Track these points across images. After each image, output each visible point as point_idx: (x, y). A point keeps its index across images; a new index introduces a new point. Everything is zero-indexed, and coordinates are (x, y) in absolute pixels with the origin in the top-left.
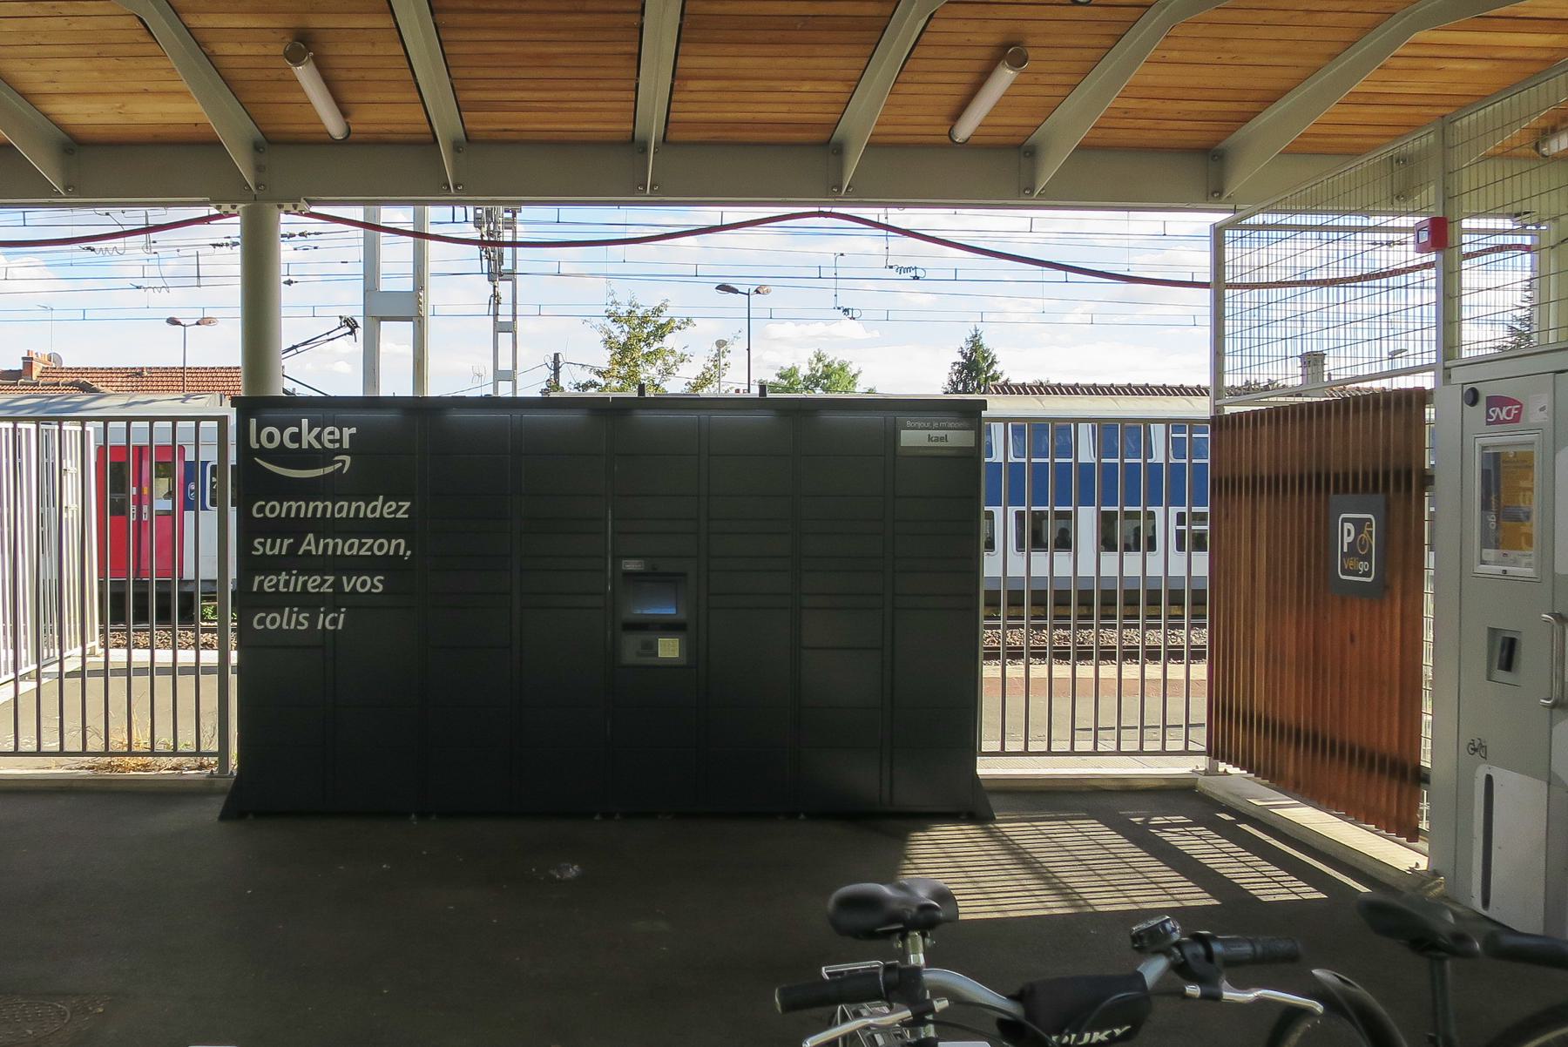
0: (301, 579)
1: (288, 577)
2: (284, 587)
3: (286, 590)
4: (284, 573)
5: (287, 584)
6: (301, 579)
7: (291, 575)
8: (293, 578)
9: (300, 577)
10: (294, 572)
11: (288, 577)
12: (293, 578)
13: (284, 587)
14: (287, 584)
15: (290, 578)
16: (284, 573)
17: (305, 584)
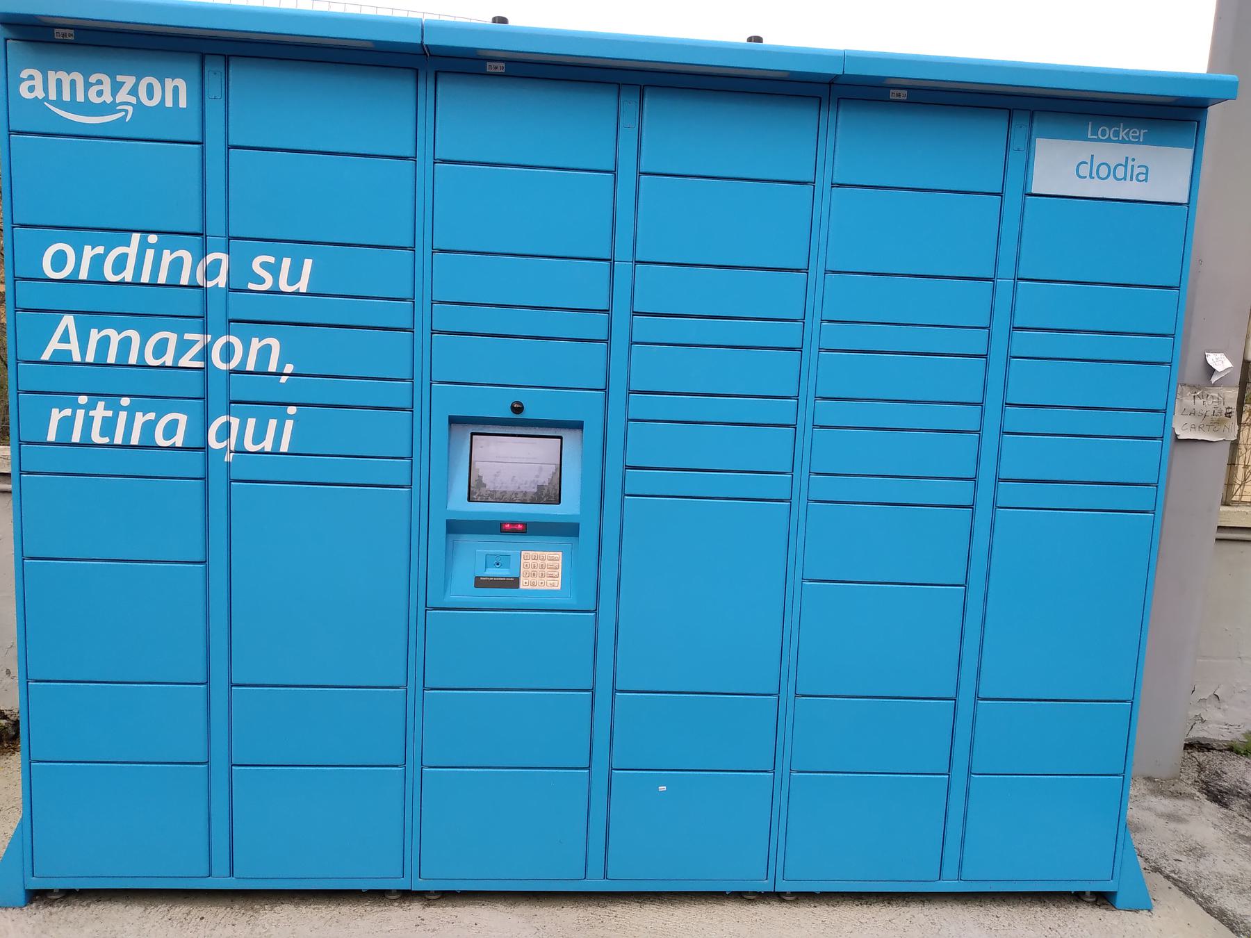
0: (140, 419)
1: (109, 413)
2: (102, 435)
3: (106, 440)
4: (101, 404)
5: (109, 426)
6: (140, 419)
7: (117, 409)
8: (123, 416)
9: (139, 415)
10: (125, 401)
11: (109, 413)
12: (123, 416)
13: (102, 435)
14: (109, 426)
15: (116, 417)
16: (101, 404)
17: (149, 427)
